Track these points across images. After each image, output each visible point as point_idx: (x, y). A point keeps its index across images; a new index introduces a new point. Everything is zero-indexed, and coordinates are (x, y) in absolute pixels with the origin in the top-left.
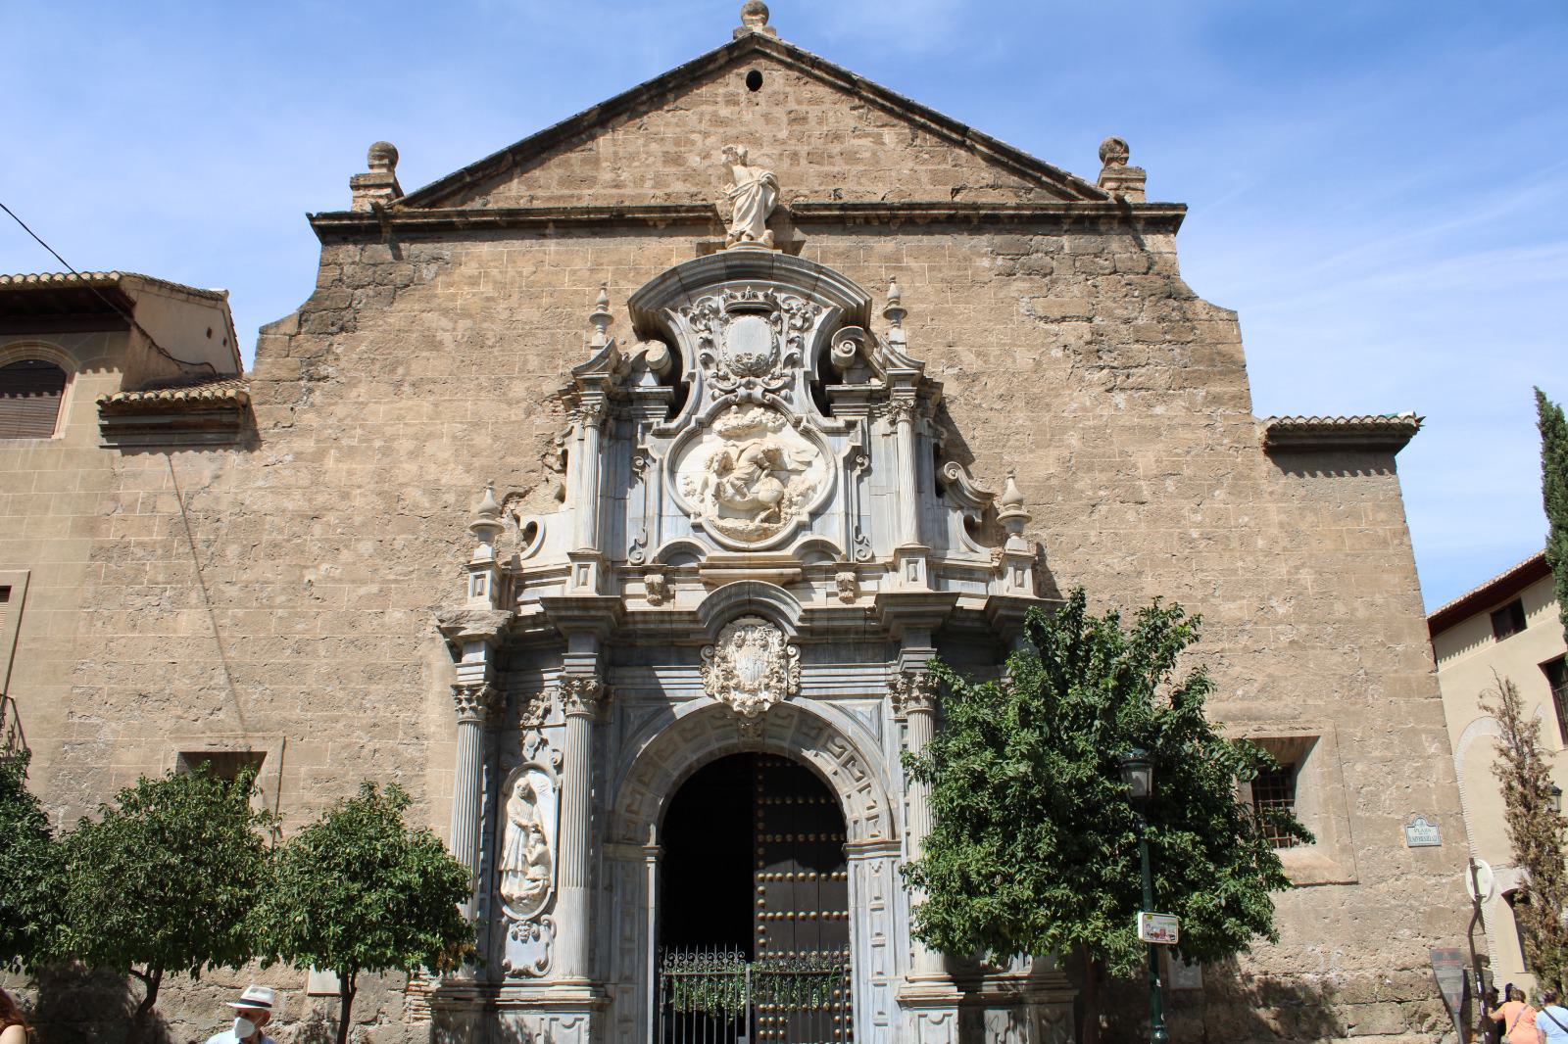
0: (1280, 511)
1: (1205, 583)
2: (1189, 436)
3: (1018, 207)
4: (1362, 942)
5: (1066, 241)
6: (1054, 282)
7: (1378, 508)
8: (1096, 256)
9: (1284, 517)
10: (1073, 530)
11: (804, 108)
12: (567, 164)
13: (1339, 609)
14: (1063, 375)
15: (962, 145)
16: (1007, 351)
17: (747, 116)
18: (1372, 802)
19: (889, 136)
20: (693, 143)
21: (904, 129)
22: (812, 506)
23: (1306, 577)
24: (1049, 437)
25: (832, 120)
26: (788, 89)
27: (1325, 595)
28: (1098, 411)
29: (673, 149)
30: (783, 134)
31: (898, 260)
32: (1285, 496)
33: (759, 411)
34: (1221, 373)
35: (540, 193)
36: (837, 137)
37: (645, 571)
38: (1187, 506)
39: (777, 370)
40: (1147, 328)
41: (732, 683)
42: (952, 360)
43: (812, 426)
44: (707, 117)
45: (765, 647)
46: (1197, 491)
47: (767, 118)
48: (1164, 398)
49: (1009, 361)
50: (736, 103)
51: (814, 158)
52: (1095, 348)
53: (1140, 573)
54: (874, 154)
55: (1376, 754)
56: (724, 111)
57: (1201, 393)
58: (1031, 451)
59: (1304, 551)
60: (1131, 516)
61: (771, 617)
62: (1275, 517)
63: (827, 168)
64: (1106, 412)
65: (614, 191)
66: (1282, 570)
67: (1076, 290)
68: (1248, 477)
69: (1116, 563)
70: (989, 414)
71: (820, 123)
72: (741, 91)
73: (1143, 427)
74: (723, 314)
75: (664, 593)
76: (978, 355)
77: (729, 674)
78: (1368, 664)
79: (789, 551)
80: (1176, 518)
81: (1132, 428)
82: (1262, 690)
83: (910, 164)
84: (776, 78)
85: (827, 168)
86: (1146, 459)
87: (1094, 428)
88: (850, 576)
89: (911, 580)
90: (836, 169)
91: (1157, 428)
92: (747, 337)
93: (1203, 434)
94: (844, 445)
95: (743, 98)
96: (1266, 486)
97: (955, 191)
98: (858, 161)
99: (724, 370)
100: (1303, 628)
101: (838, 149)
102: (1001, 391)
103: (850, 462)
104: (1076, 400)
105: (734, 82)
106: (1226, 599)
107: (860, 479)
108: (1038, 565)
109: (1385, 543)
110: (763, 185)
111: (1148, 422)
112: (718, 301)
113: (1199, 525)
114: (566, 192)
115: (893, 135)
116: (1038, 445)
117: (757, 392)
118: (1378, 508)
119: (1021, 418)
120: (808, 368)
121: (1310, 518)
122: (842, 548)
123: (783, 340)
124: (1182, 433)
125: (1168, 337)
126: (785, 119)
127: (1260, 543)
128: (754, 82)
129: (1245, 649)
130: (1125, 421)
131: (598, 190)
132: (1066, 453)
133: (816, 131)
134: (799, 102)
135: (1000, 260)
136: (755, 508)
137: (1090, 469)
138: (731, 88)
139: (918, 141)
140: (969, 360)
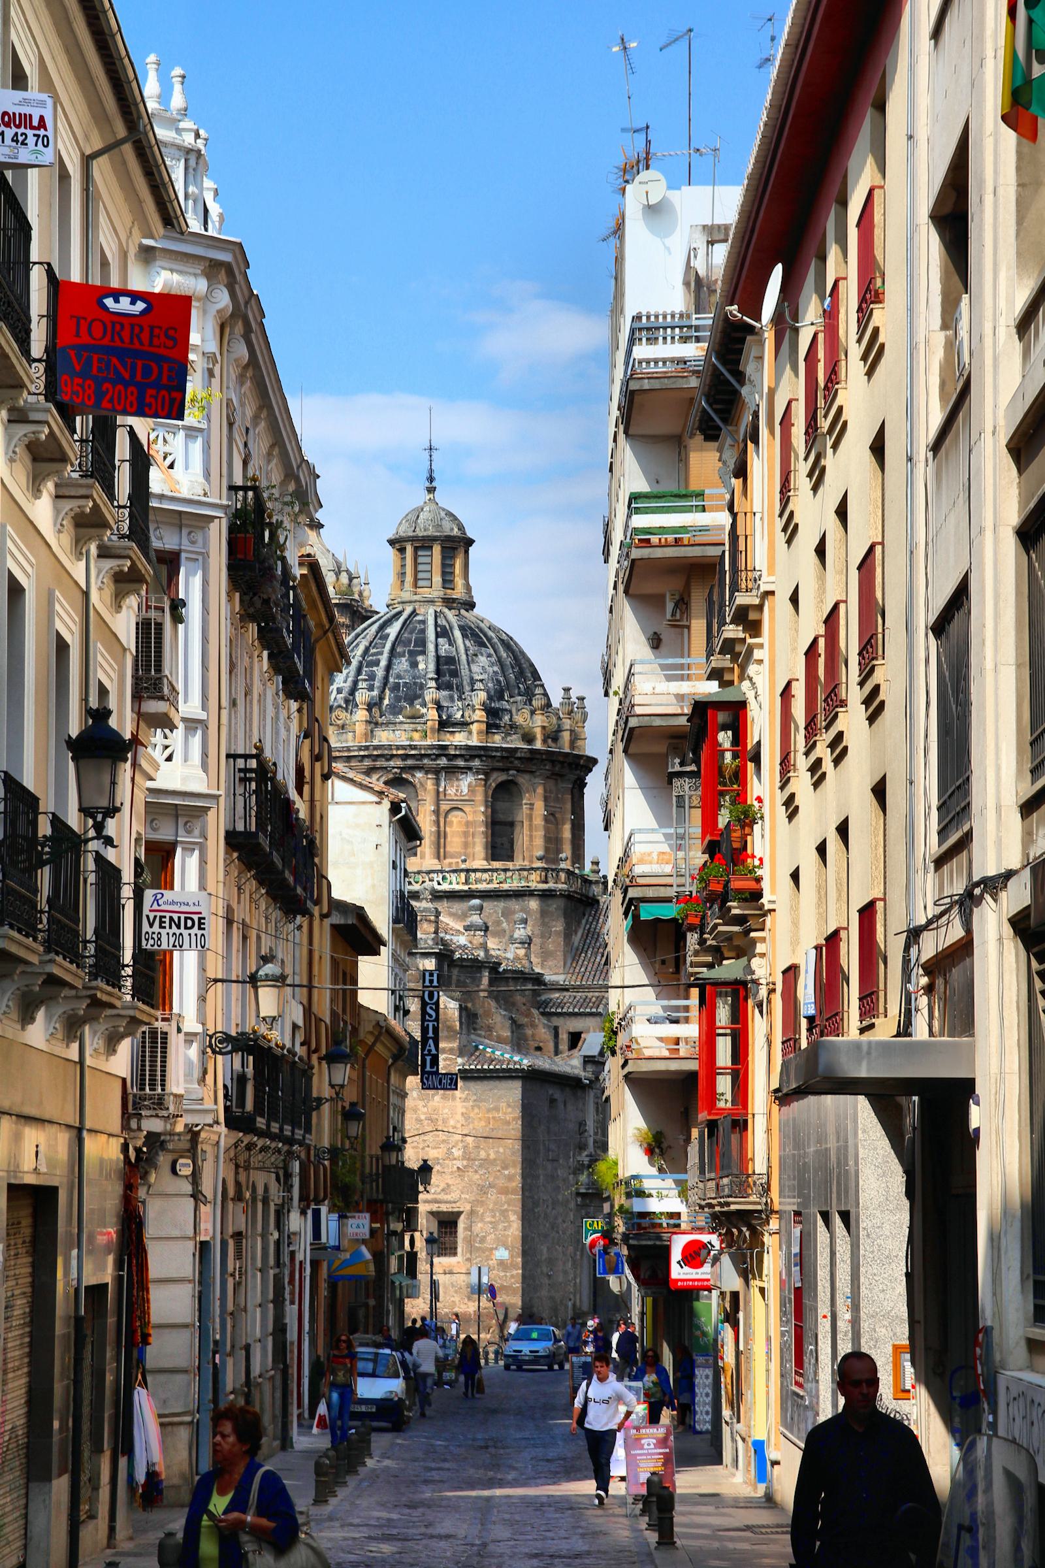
7: (509, 1106)
9: (464, 1110)
18: (483, 1240)
27: (477, 1147)
32: (466, 1100)
38: (421, 1103)
55: (488, 1219)
59: (471, 1126)
78: (491, 1179)
82: (443, 1190)
100: (465, 1163)
109: (508, 1123)
118: (509, 1106)
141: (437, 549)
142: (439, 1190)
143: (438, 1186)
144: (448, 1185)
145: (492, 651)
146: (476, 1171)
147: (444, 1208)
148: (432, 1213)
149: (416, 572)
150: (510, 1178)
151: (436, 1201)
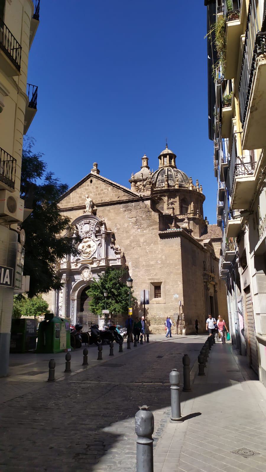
0: (161, 247)
1: (148, 259)
2: (149, 235)
3: (126, 200)
4: (165, 312)
5: (133, 204)
6: (131, 212)
7: (176, 245)
8: (138, 206)
9: (161, 248)
10: (131, 252)
11: (98, 185)
12: (66, 199)
13: (168, 262)
14: (131, 227)
15: (119, 189)
16: (124, 224)
17: (90, 188)
18: (169, 291)
19: (110, 189)
20: (82, 194)
21: (112, 186)
22: (94, 252)
23: (164, 257)
24: (128, 238)
25: (101, 187)
26: (96, 182)
27: (166, 260)
28: (135, 233)
29: (80, 195)
30: (95, 191)
31: (110, 211)
32: (162, 244)
33: (88, 238)
34: (155, 224)
35: (63, 205)
36: (102, 190)
37: (74, 262)
39: (90, 232)
40: (144, 218)
41: (84, 277)
42: (116, 226)
43: (94, 240)
44: (85, 189)
45: (88, 272)
46: (149, 244)
47: (93, 188)
48: (145, 229)
49: (124, 225)
50: (89, 186)
51: (99, 194)
52: (136, 222)
53: (139, 258)
54: (107, 192)
55: (171, 284)
56: (87, 188)
57: (151, 228)
58: (126, 240)
59: (164, 253)
60: (139, 249)
61: (88, 268)
62: (160, 248)
63: (101, 196)
64: (137, 233)
65: (73, 204)
66: (160, 256)
67: (134, 213)
68: (156, 241)
69: (136, 256)
70: (121, 234)
71: (100, 188)
72: (89, 184)
73: (142, 235)
74: (84, 224)
75: (76, 265)
76: (120, 225)
77: (83, 276)
78: (171, 270)
79: (91, 259)
80: (145, 249)
81: (140, 235)
82: (155, 275)
83: (112, 193)
84: (94, 180)
85: (101, 196)
86: (142, 240)
87: (135, 235)
88: (98, 262)
89: (103, 263)
90: (102, 196)
91: (144, 235)
92: (86, 228)
93: (151, 235)
94: (99, 242)
95: (90, 185)
96: (159, 243)
97: (118, 197)
98: (105, 194)
99: (84, 233)
100: (162, 265)
101: (102, 192)
102: (123, 231)
103: (99, 245)
104: (133, 231)
105: (88, 181)
106: (151, 261)
107: (100, 247)
108: (123, 258)
110: (90, 202)
111: (143, 234)
112: (83, 222)
113: (148, 250)
114: (66, 204)
115: (110, 188)
116: (127, 239)
117: (87, 236)
118: (176, 245)
119: (125, 235)
120: (94, 232)
121: (165, 247)
122: (97, 258)
123: (91, 227)
124: (148, 235)
125: (147, 219)
126: (95, 188)
127: (157, 252)
128: (91, 181)
129: (153, 269)
130: (139, 234)
131: (71, 204)
132: (130, 240)
133: (99, 189)
134: (97, 184)
135: (124, 209)
136: (87, 253)
137: (134, 242)
138: (88, 183)
139: (114, 189)
140: (119, 226)
141: (168, 156)
142: (153, 275)
143: (153, 274)
144: (157, 273)
145: (180, 174)
146: (166, 268)
147: (156, 281)
148: (151, 283)
149: (164, 162)
150: (178, 269)
151: (152, 279)
